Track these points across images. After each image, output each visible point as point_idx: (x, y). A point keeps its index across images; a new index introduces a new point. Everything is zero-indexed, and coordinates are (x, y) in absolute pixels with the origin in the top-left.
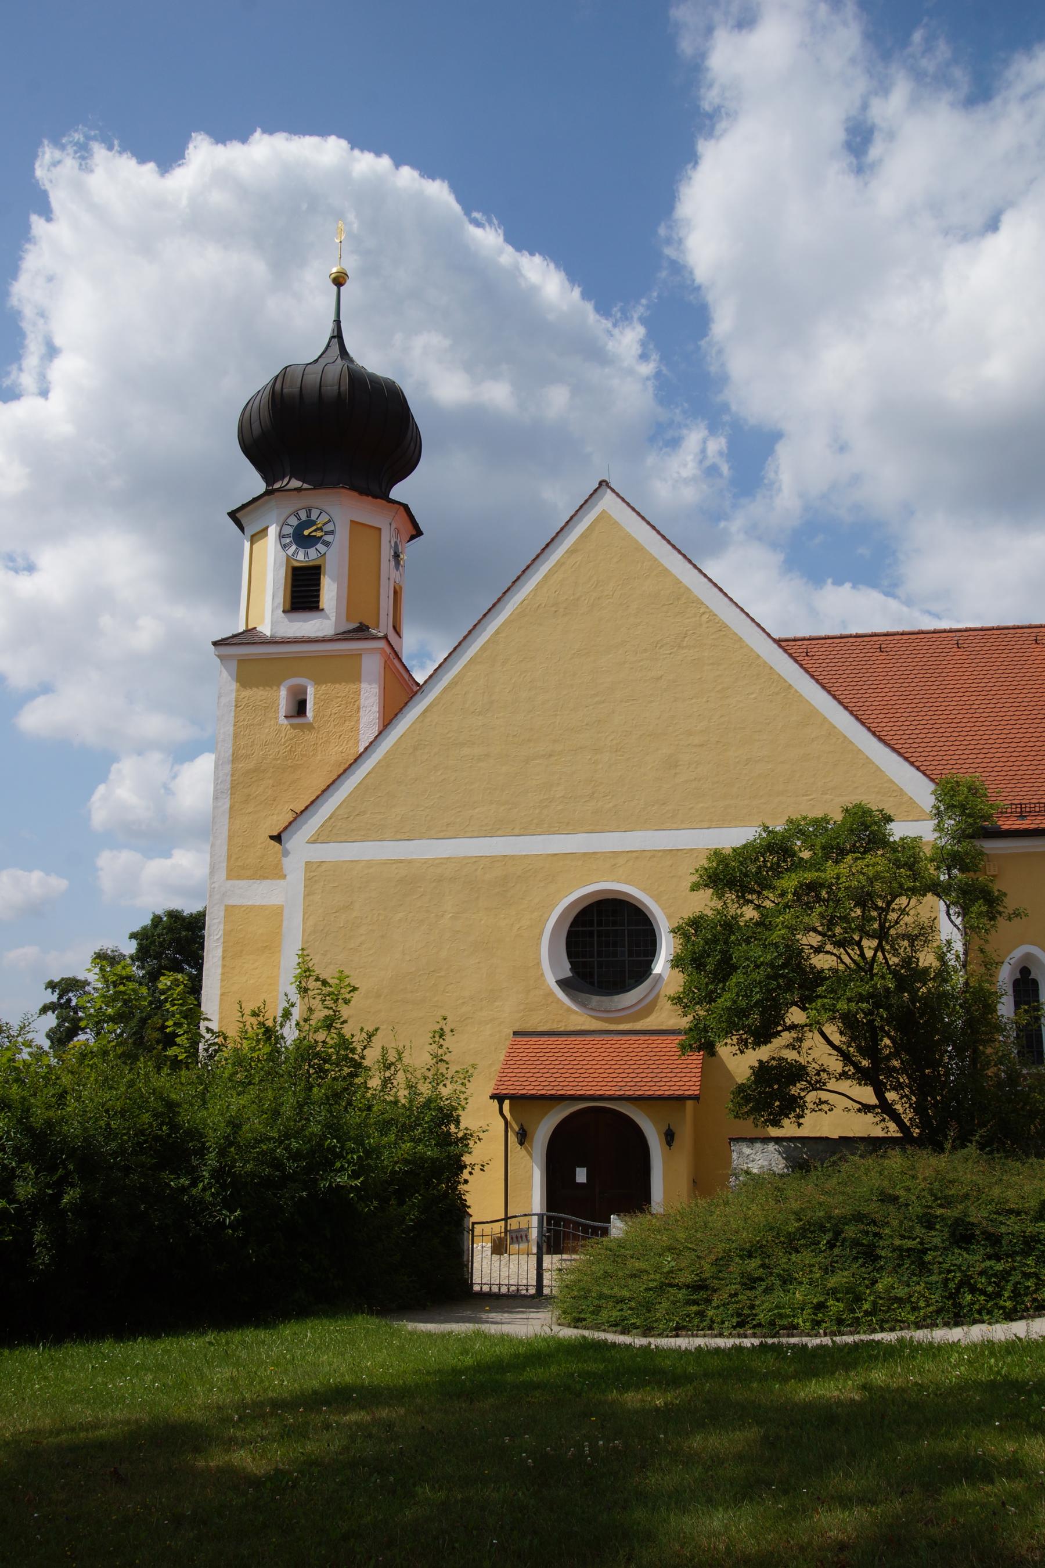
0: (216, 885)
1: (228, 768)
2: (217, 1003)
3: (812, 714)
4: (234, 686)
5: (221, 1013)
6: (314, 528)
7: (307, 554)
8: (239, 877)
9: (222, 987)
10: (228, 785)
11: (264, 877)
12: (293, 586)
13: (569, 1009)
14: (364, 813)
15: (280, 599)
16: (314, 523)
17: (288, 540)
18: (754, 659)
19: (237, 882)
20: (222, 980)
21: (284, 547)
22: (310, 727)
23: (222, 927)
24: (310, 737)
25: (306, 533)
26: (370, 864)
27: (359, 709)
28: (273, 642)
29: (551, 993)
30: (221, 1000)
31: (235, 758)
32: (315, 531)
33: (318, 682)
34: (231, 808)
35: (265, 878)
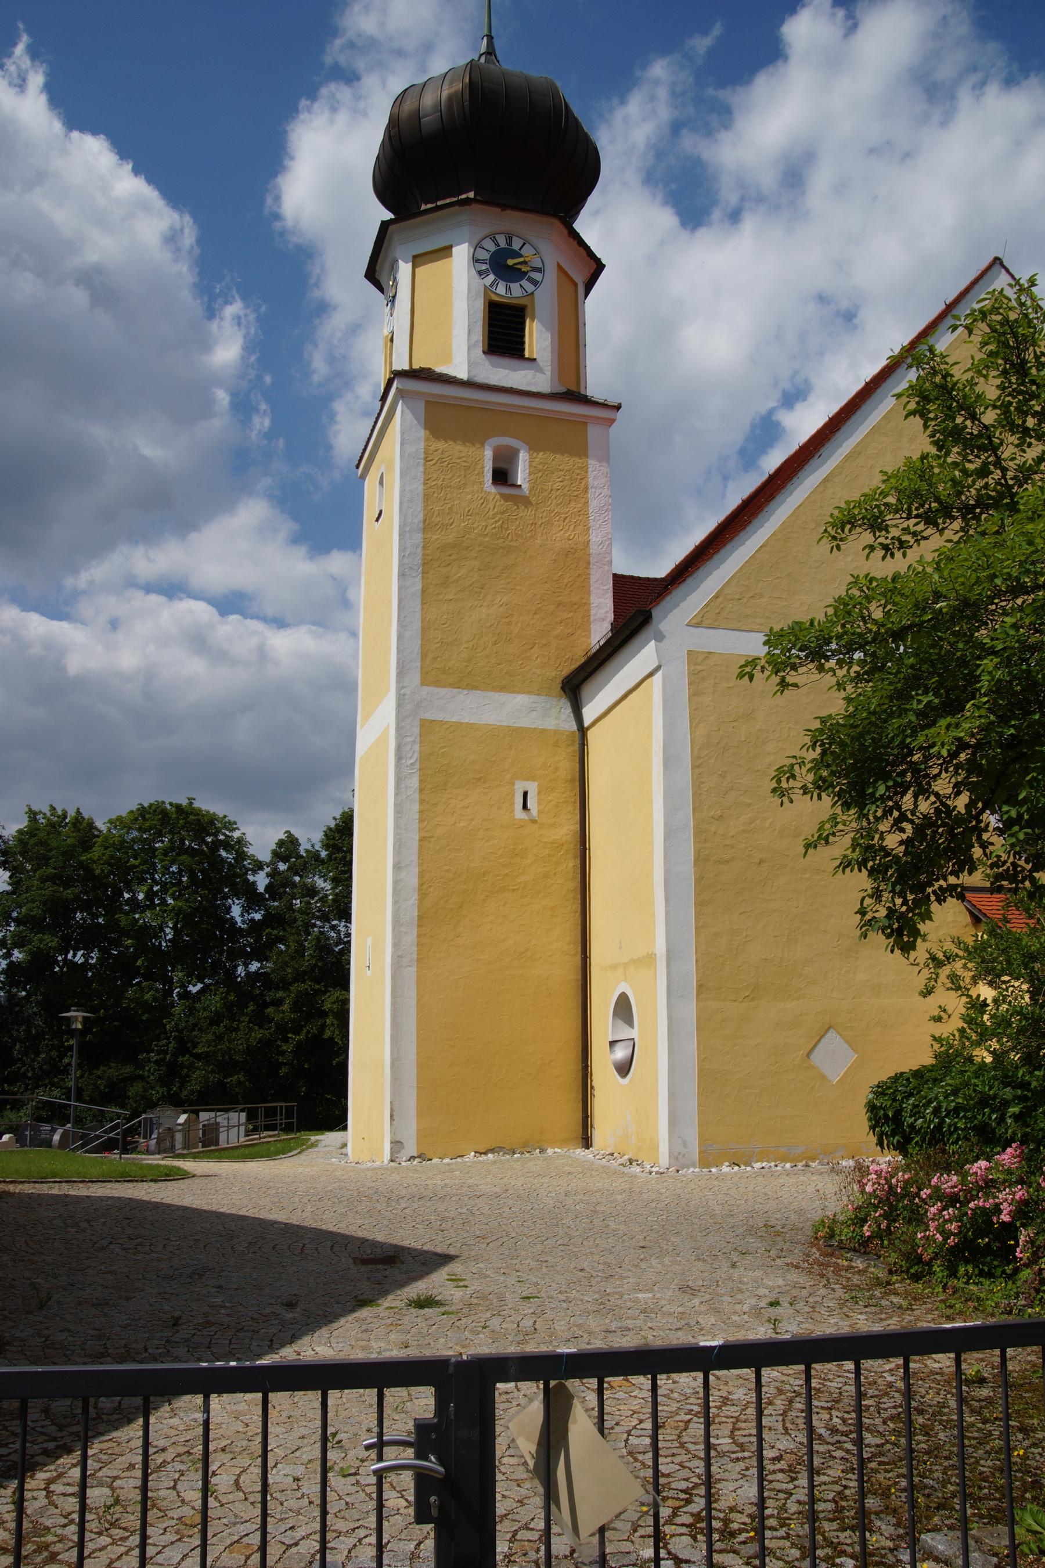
0: (407, 691)
1: (418, 538)
2: (416, 850)
4: (422, 433)
5: (420, 865)
6: (521, 260)
7: (508, 289)
8: (438, 684)
9: (420, 829)
10: (418, 560)
11: (472, 687)
12: (490, 325)
15: (479, 335)
16: (516, 254)
17: (484, 267)
19: (436, 690)
20: (421, 821)
21: (480, 273)
22: (525, 501)
23: (417, 747)
24: (527, 514)
25: (510, 262)
27: (586, 490)
28: (469, 384)
31: (427, 526)
32: (520, 263)
33: (534, 447)
34: (424, 591)
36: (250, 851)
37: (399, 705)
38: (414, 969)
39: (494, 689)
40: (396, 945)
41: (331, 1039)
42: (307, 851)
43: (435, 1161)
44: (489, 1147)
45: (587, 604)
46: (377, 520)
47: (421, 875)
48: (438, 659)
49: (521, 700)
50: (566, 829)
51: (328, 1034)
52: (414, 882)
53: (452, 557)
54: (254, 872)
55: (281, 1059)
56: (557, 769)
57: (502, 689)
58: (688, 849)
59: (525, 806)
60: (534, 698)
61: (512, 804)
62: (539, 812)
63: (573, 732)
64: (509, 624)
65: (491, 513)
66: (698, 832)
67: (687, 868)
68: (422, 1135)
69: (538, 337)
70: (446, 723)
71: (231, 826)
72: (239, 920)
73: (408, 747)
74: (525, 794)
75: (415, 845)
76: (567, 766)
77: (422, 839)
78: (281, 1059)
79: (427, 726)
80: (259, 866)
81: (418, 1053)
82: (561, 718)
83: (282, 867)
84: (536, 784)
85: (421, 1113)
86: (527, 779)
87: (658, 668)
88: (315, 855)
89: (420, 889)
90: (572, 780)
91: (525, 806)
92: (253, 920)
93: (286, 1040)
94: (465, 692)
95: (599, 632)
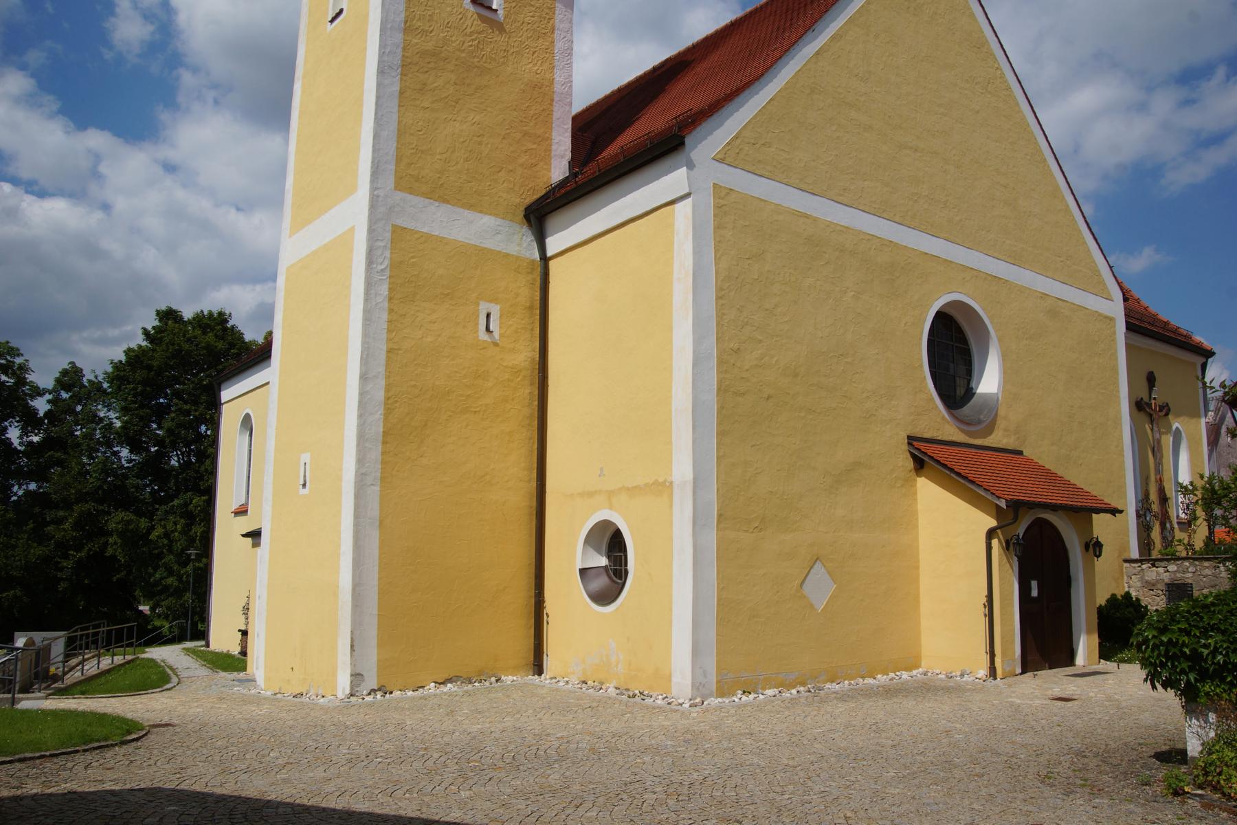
0: (381, 193)
1: (399, 37)
2: (383, 362)
5: (387, 377)
8: (411, 191)
9: (389, 340)
10: (397, 60)
11: (444, 200)
20: (389, 331)
30: (388, 358)
31: (408, 29)
34: (401, 93)
35: (448, 202)
36: (31, 377)
37: (373, 206)
38: (377, 488)
39: (464, 206)
40: (361, 461)
41: (113, 557)
42: (90, 381)
43: (397, 694)
44: (446, 676)
45: (549, 139)
46: (332, 21)
47: (388, 388)
48: (411, 166)
49: (487, 221)
50: (525, 354)
51: (109, 552)
52: (380, 395)
53: (432, 65)
54: (33, 397)
55: (59, 575)
56: (517, 295)
57: (470, 207)
58: (712, 378)
59: (488, 329)
60: (499, 221)
61: (477, 324)
62: (501, 336)
63: (533, 261)
64: (480, 143)
65: (469, 30)
66: (721, 362)
67: (711, 398)
68: (383, 666)
70: (417, 232)
71: (15, 352)
72: (16, 442)
73: (379, 252)
74: (488, 316)
75: (383, 356)
76: (527, 293)
77: (389, 351)
78: (59, 575)
79: (399, 232)
80: (38, 392)
81: (380, 579)
82: (522, 244)
83: (65, 395)
84: (498, 307)
85: (381, 645)
86: (491, 301)
87: (688, 195)
88: (96, 386)
89: (386, 404)
90: (531, 308)
91: (488, 329)
92: (31, 443)
93: (66, 557)
94: (437, 204)
95: (558, 170)
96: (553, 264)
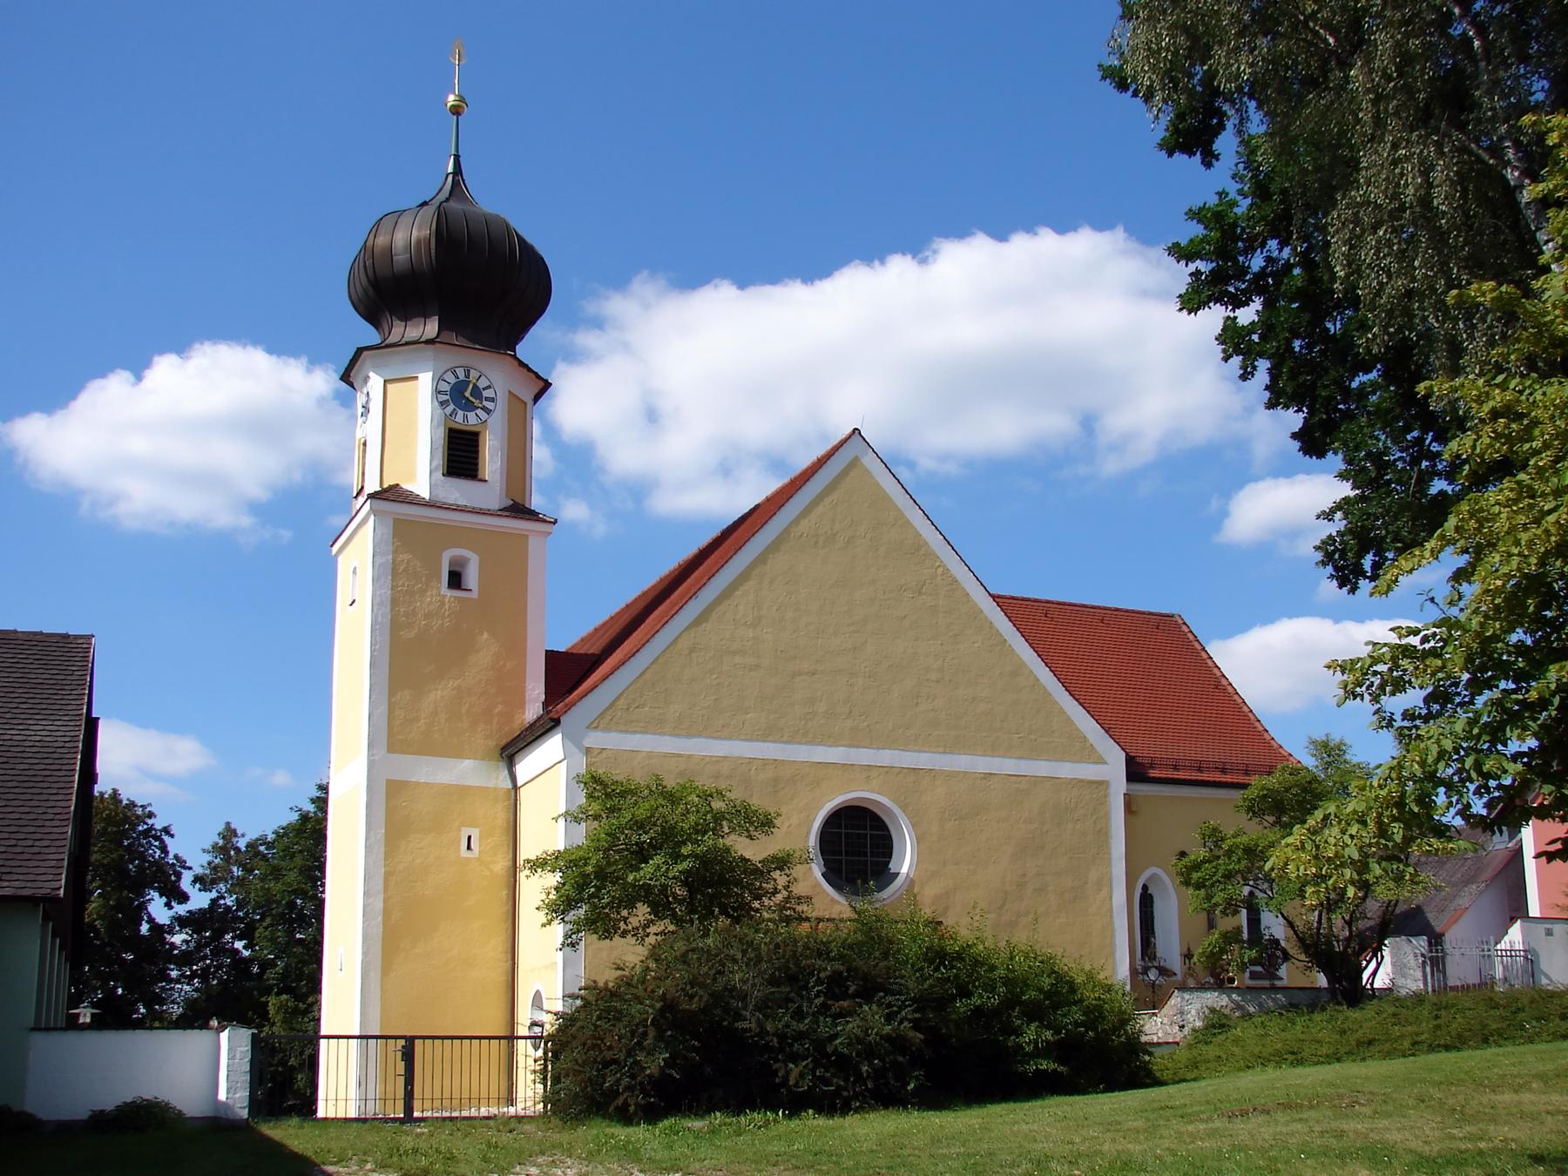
3: (1020, 668)
13: (833, 900)
14: (643, 706)
15: (440, 460)
18: (976, 612)
26: (650, 755)
29: (818, 885)
49: (468, 764)
69: (492, 458)
76: (501, 816)
82: (502, 781)
96: (523, 792)
